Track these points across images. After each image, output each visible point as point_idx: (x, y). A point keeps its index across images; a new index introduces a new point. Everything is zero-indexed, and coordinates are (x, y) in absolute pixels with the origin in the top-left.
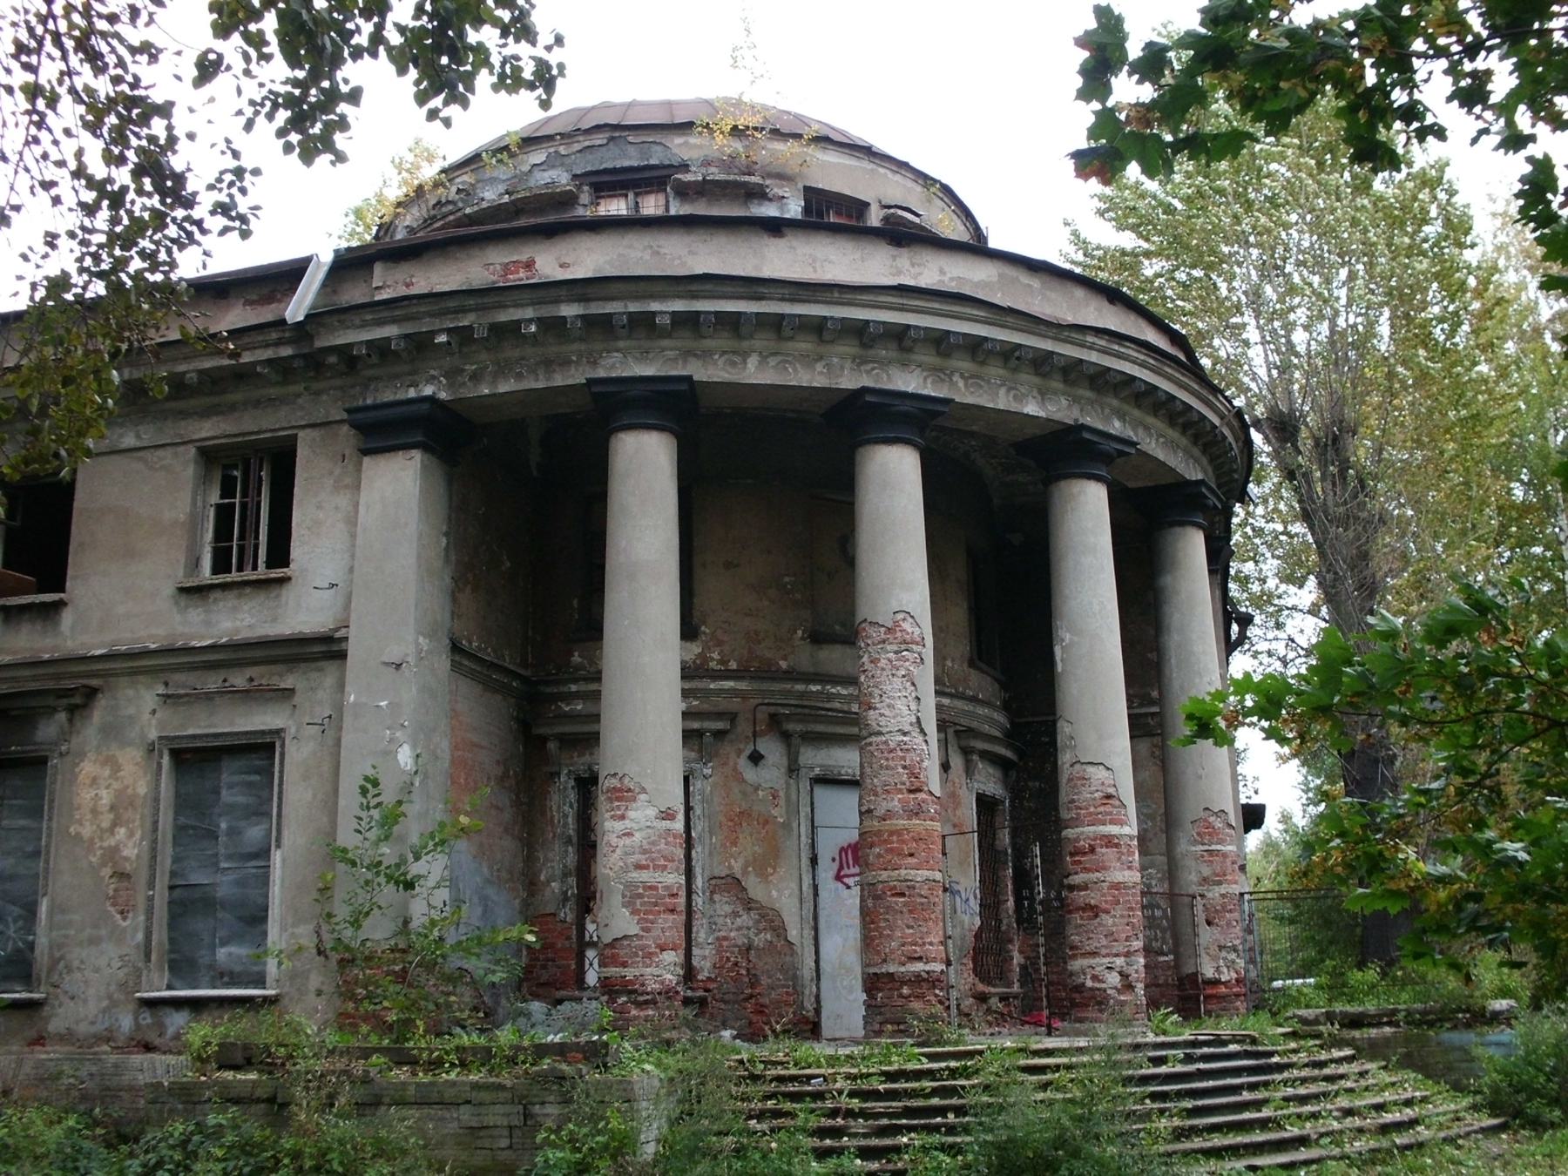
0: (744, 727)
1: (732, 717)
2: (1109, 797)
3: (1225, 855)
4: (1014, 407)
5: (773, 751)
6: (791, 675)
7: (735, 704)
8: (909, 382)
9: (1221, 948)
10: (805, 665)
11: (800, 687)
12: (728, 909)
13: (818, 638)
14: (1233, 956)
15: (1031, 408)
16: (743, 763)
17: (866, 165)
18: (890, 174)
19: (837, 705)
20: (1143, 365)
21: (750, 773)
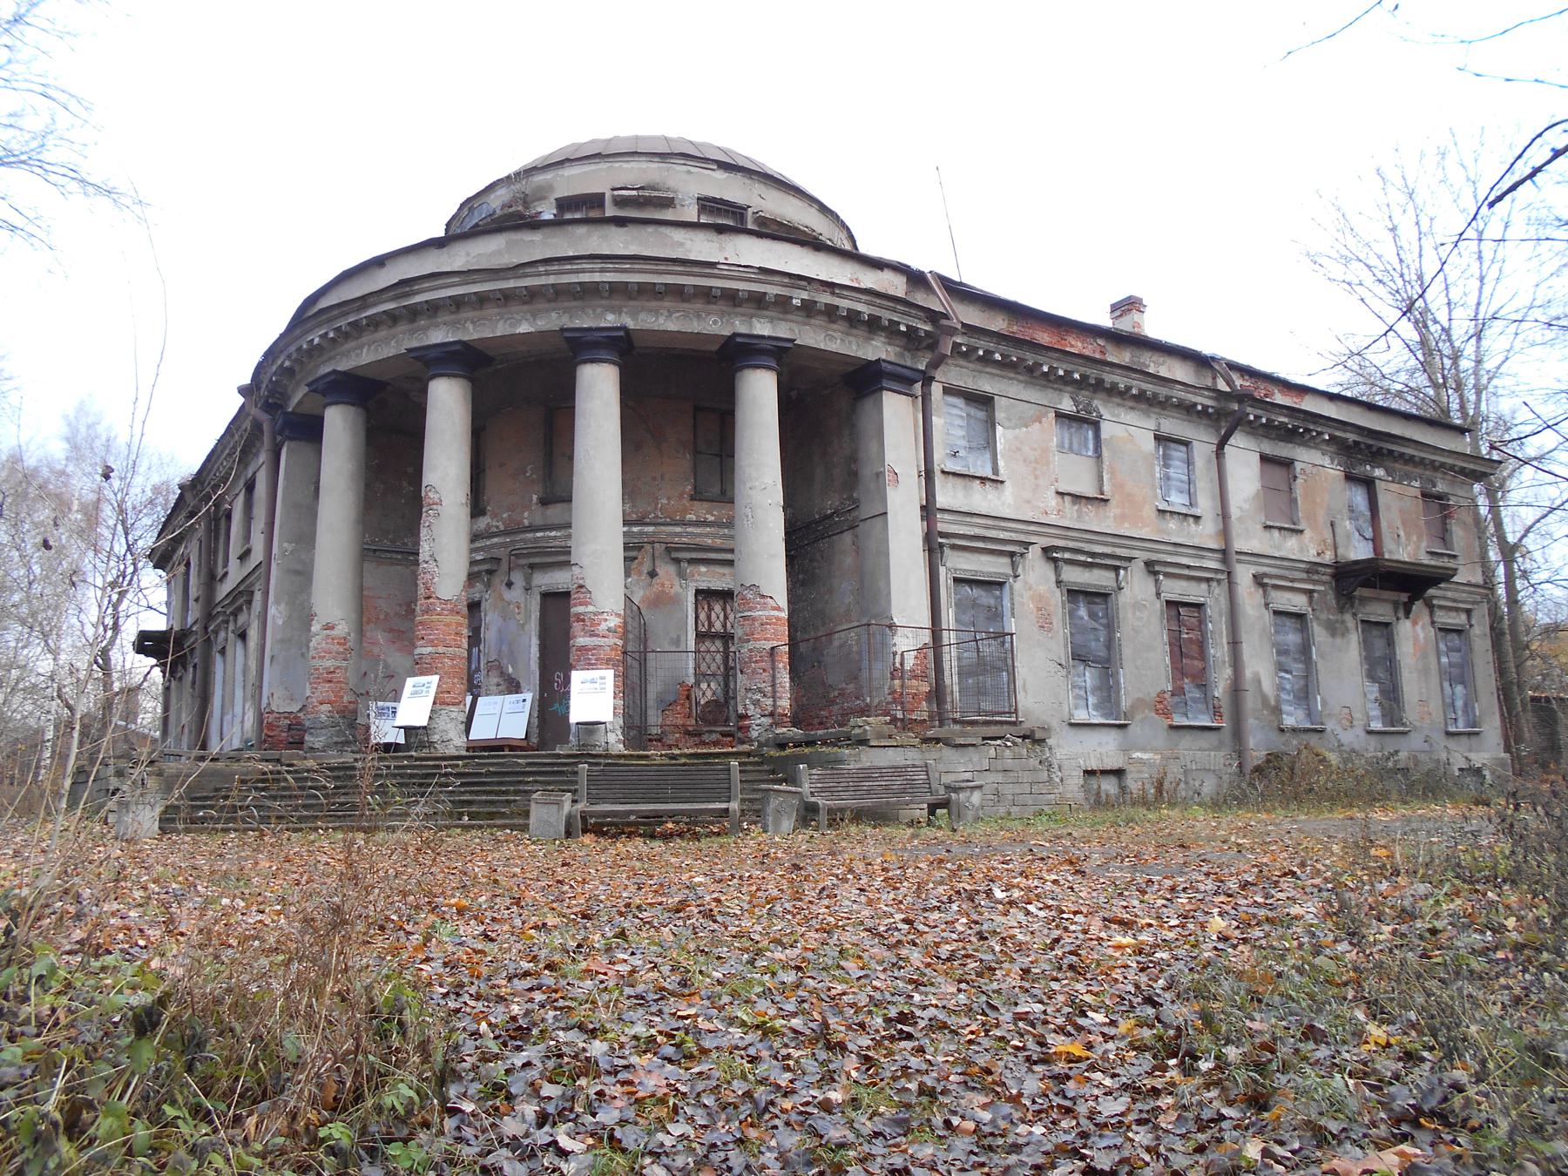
0: (504, 565)
1: (498, 560)
2: (581, 586)
3: (754, 619)
4: (509, 331)
5: (518, 578)
6: (532, 529)
7: (496, 553)
8: (439, 336)
9: (748, 690)
10: (539, 521)
11: (530, 535)
12: (496, 680)
13: (544, 502)
14: (758, 696)
15: (524, 328)
16: (504, 587)
17: (603, 166)
18: (625, 165)
19: (557, 543)
20: (602, 271)
21: (508, 595)
